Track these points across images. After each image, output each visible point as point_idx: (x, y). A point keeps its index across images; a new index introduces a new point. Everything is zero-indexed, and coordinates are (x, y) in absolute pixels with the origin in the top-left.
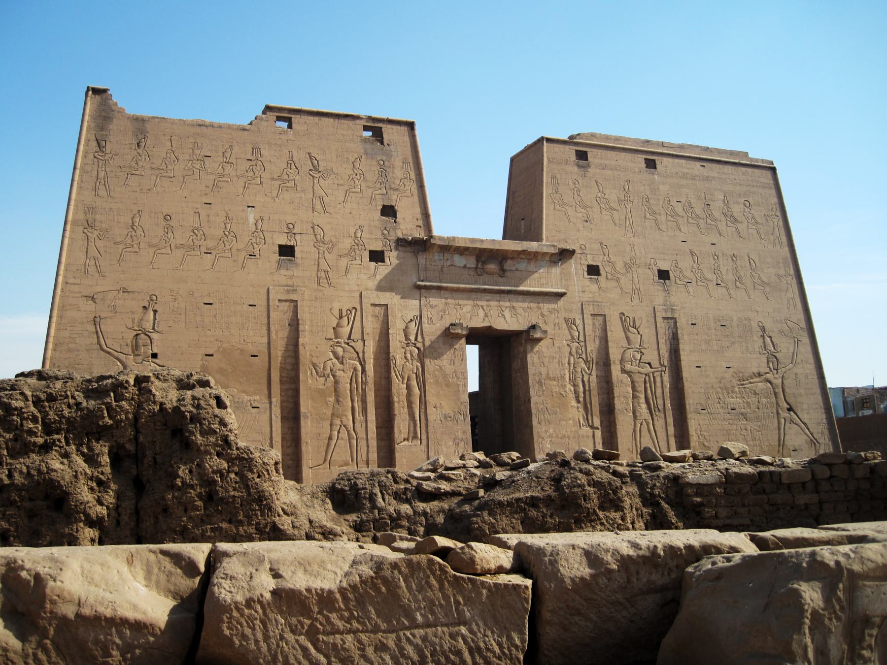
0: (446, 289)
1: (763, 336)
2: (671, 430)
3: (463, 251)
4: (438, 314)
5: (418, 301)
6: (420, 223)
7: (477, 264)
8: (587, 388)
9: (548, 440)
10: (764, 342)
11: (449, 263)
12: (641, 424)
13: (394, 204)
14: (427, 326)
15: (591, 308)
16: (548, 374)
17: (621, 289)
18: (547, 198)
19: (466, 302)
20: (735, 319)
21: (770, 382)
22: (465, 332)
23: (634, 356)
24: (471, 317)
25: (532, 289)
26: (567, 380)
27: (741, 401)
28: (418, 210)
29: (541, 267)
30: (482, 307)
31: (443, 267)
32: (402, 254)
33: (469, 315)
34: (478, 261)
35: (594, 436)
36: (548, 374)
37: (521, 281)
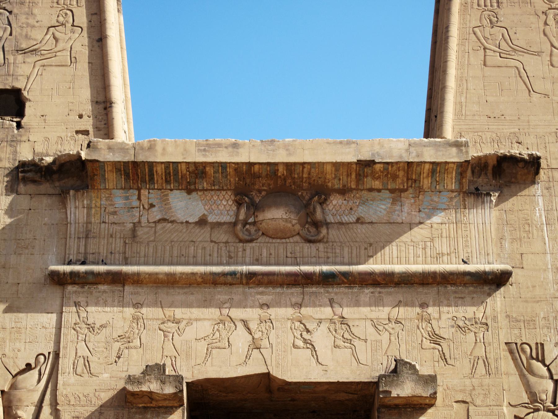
0: (136, 280)
3: (192, 177)
4: (108, 346)
5: (54, 317)
6: (88, 124)
7: (237, 215)
11: (155, 214)
13: (18, 85)
14: (73, 379)
18: (463, 40)
19: (196, 312)
22: (169, 390)
24: (208, 353)
25: (398, 268)
28: (84, 94)
29: (434, 210)
30: (245, 323)
31: (136, 225)
32: (24, 202)
33: (202, 347)
34: (239, 204)
37: (371, 249)
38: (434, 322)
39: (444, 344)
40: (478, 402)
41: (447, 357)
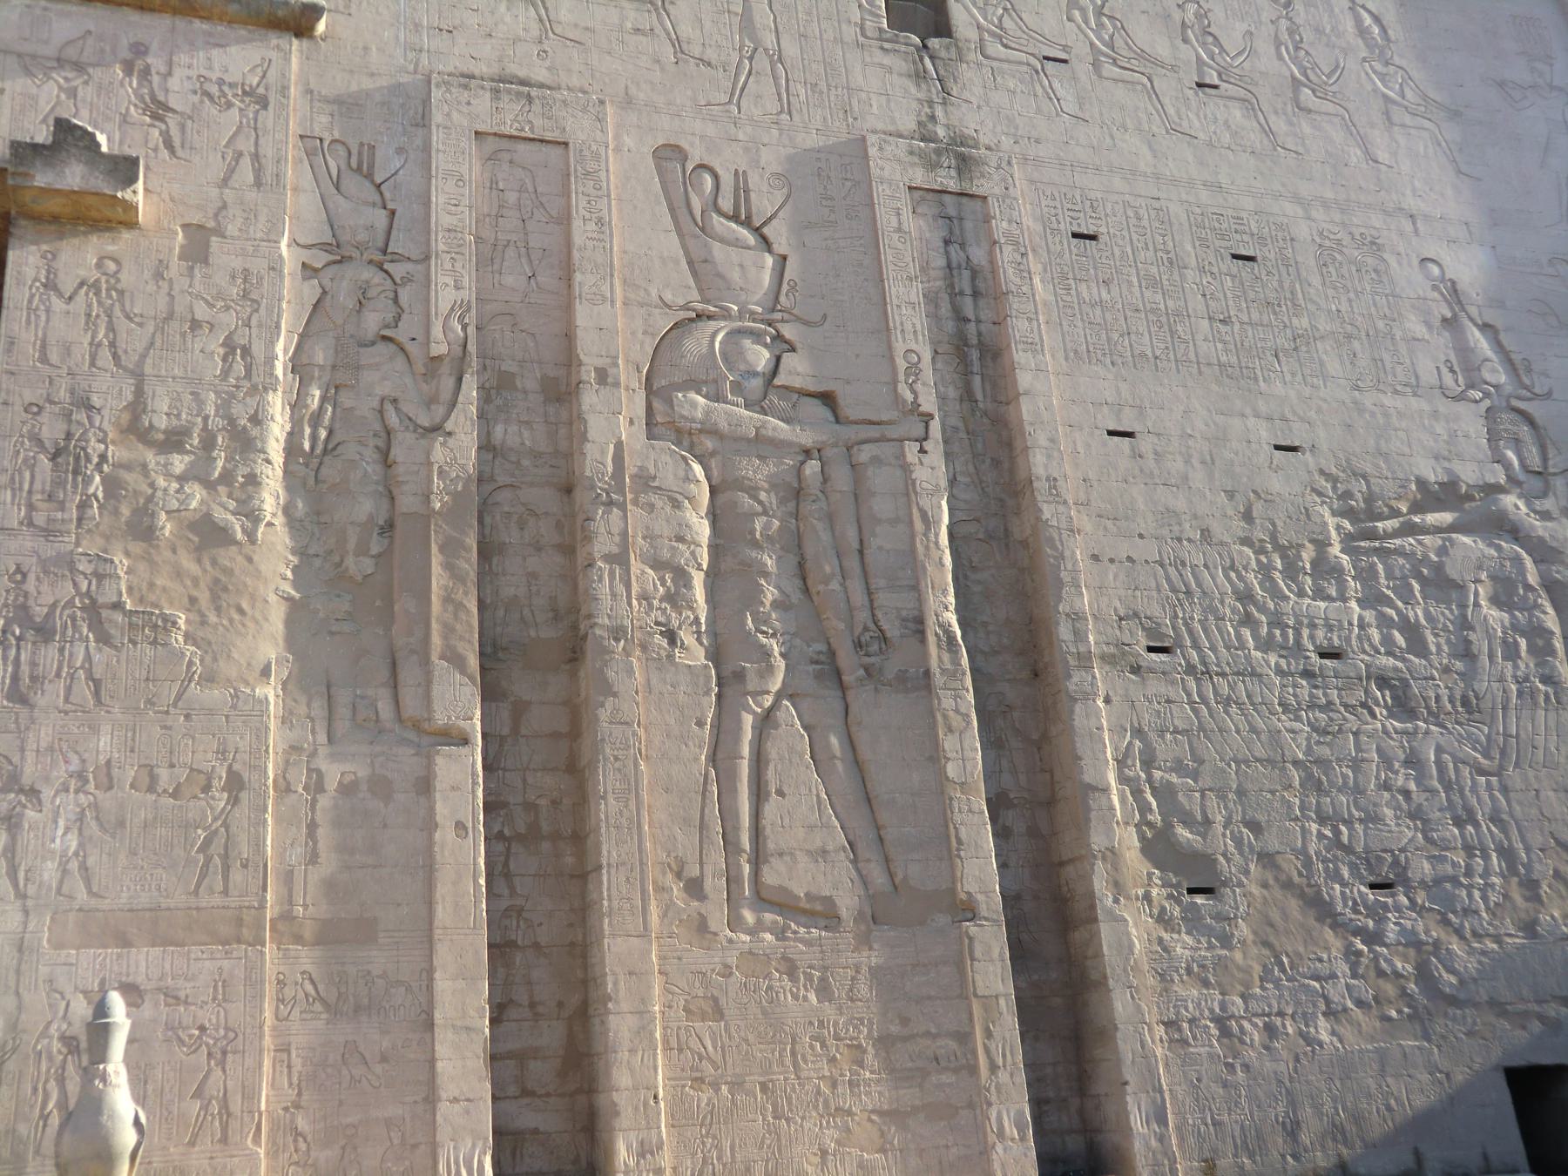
1: (1449, 323)
2: (966, 755)
8: (407, 502)
9: (69, 804)
10: (1464, 349)
12: (767, 720)
15: (483, 102)
16: (138, 406)
17: (677, 43)
20: (1303, 231)
21: (1515, 532)
23: (732, 354)
26: (275, 450)
27: (1369, 616)
35: (425, 786)
36: (138, 406)
38: (156, 79)
39: (172, 121)
40: (231, 230)
41: (177, 142)
